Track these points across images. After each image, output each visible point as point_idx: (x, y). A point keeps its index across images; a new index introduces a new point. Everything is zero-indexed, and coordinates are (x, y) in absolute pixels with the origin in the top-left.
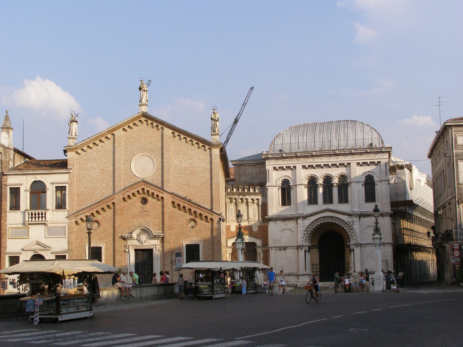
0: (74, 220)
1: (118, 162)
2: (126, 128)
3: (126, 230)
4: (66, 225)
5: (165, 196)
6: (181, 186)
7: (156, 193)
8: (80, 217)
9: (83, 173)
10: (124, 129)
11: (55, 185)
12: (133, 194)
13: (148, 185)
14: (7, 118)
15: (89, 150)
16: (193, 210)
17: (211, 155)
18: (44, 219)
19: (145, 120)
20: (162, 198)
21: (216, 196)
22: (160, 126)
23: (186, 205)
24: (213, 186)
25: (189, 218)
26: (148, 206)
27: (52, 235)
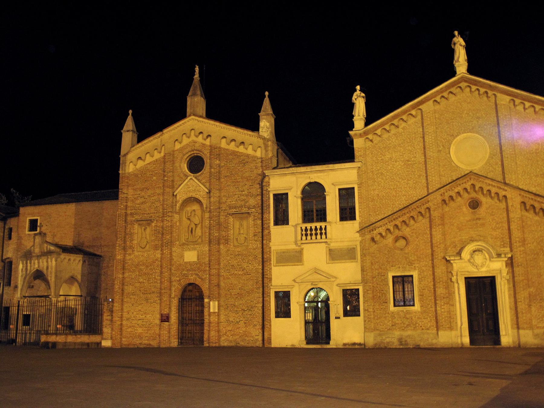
0: (368, 237)
1: (431, 147)
3: (450, 249)
4: (358, 243)
5: (510, 193)
7: (494, 190)
8: (377, 230)
9: (379, 168)
10: (435, 101)
15: (386, 135)
18: (324, 236)
20: (505, 197)
22: (490, 93)
26: (482, 211)
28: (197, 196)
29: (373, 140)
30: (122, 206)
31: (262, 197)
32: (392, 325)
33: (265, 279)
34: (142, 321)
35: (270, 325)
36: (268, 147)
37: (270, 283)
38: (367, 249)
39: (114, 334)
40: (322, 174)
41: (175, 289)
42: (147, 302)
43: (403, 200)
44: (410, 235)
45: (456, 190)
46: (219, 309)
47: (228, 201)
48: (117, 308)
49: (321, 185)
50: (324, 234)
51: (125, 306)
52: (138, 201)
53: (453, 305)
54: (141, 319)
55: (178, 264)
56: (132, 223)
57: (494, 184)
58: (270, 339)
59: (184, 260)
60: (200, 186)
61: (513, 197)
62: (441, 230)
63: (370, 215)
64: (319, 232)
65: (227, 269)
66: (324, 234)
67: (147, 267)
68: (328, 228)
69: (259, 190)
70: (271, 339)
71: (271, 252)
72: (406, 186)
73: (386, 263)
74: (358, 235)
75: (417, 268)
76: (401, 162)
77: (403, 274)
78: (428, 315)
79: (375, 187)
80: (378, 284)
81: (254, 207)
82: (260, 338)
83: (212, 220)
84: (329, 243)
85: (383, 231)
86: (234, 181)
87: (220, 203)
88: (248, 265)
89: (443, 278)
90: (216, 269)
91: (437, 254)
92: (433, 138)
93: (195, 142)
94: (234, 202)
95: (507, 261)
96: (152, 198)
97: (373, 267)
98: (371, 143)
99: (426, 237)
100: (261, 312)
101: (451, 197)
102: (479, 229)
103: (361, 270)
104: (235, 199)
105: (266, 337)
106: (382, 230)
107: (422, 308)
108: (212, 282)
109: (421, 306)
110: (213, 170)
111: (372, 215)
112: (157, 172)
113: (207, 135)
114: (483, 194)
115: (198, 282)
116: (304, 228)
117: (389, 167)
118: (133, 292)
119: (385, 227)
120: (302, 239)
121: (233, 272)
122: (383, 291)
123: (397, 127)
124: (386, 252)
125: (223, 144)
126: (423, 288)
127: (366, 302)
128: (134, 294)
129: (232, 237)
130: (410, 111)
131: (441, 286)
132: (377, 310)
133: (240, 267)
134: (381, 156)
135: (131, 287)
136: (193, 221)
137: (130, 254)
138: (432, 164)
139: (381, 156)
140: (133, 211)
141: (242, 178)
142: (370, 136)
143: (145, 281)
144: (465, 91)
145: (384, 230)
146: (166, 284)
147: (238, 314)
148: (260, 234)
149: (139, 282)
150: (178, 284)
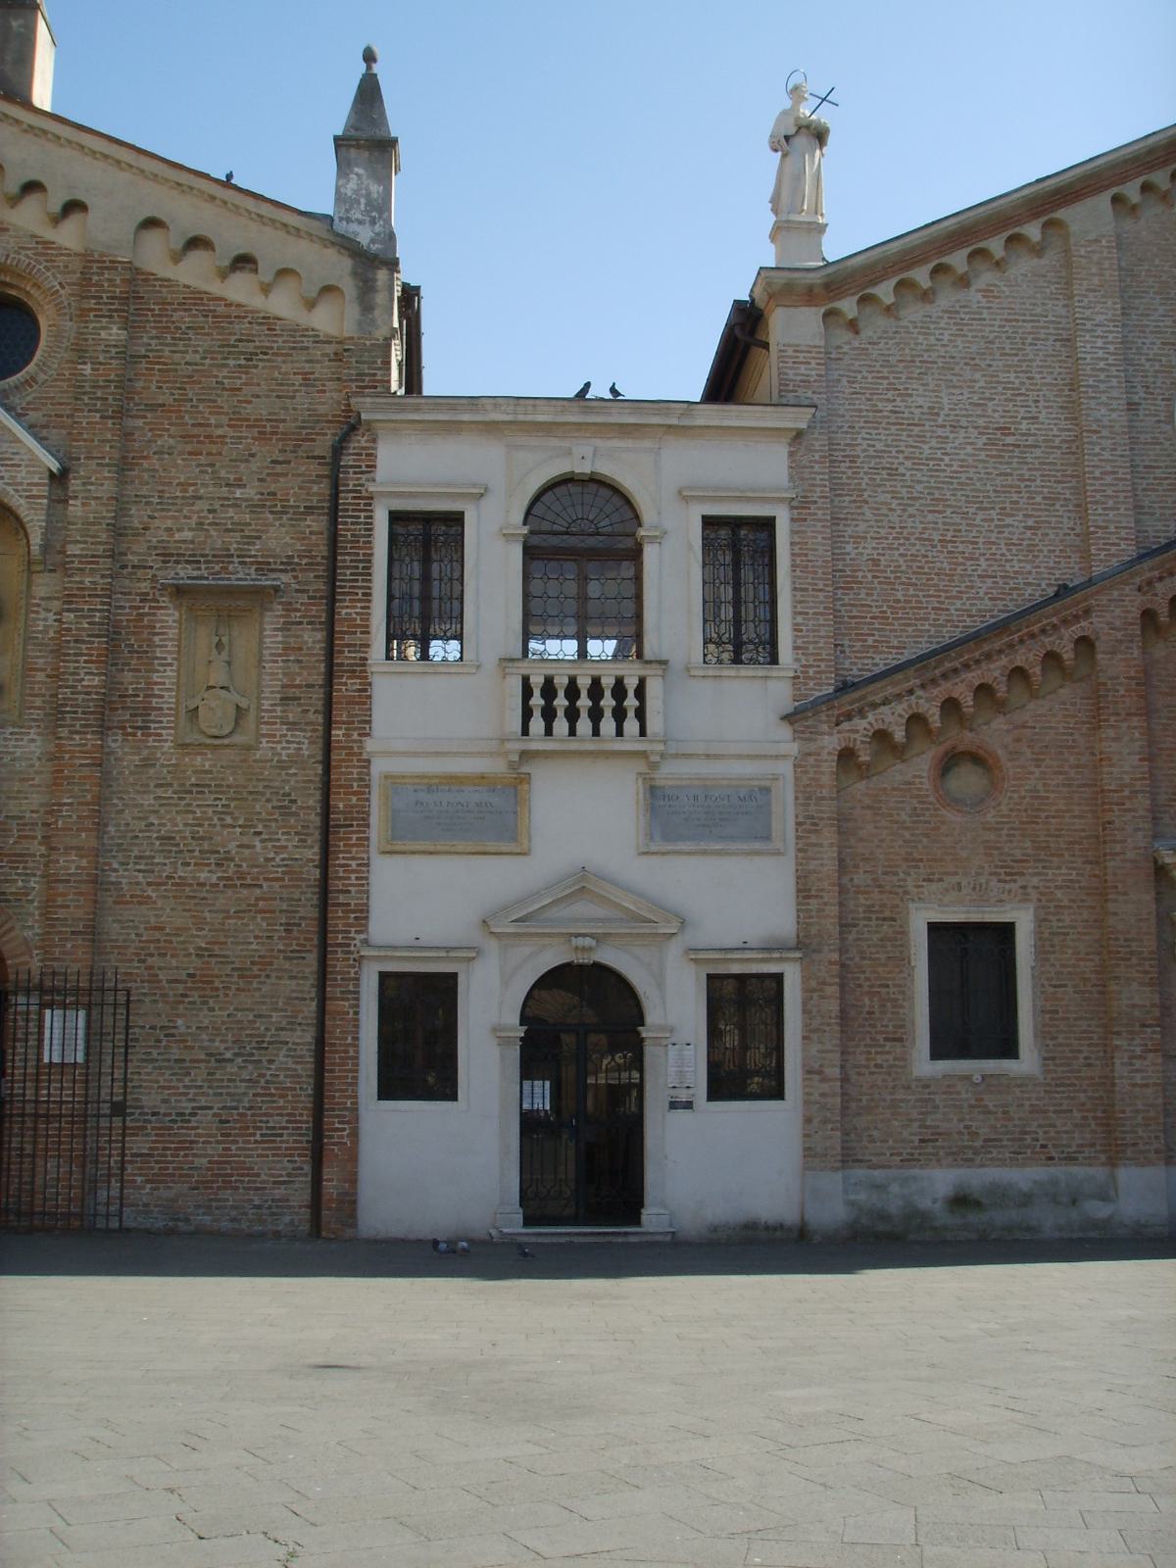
0: (831, 743)
1: (1102, 386)
4: (786, 769)
8: (871, 717)
9: (879, 446)
14: (369, 94)
18: (631, 725)
29: (861, 324)
31: (334, 521)
32: (922, 1141)
33: (336, 915)
35: (355, 1134)
36: (377, 291)
37: (357, 932)
38: (823, 798)
40: (629, 443)
43: (981, 594)
44: (1006, 747)
46: (87, 1054)
47: (157, 523)
49: (615, 490)
50: (631, 714)
58: (349, 1203)
60: (20, 441)
63: (836, 645)
64: (608, 702)
65: (136, 852)
66: (631, 714)
68: (653, 689)
69: (315, 488)
70: (355, 1202)
71: (368, 786)
72: (993, 537)
74: (785, 732)
75: (1034, 895)
76: (973, 433)
77: (975, 918)
78: (1072, 1098)
80: (864, 958)
82: (299, 1194)
83: (69, 610)
84: (653, 758)
86: (196, 431)
87: (118, 531)
88: (245, 840)
89: (1141, 940)
90: (78, 848)
91: (1118, 838)
92: (1111, 348)
94: (187, 535)
97: (845, 880)
99: (1072, 760)
100: (306, 1069)
103: (798, 891)
104: (195, 518)
105: (331, 1186)
106: (893, 718)
108: (61, 914)
111: (847, 650)
113: (67, 197)
116: (537, 681)
117: (926, 447)
119: (905, 705)
120: (525, 731)
121: (168, 870)
122: (888, 986)
124: (904, 817)
125: (154, 255)
126: (1054, 982)
127: (815, 1036)
129: (169, 699)
130: (1019, 223)
132: (859, 1074)
133: (206, 846)
134: (890, 395)
138: (1107, 455)
139: (890, 395)
142: (848, 306)
145: (900, 715)
148: (318, 695)
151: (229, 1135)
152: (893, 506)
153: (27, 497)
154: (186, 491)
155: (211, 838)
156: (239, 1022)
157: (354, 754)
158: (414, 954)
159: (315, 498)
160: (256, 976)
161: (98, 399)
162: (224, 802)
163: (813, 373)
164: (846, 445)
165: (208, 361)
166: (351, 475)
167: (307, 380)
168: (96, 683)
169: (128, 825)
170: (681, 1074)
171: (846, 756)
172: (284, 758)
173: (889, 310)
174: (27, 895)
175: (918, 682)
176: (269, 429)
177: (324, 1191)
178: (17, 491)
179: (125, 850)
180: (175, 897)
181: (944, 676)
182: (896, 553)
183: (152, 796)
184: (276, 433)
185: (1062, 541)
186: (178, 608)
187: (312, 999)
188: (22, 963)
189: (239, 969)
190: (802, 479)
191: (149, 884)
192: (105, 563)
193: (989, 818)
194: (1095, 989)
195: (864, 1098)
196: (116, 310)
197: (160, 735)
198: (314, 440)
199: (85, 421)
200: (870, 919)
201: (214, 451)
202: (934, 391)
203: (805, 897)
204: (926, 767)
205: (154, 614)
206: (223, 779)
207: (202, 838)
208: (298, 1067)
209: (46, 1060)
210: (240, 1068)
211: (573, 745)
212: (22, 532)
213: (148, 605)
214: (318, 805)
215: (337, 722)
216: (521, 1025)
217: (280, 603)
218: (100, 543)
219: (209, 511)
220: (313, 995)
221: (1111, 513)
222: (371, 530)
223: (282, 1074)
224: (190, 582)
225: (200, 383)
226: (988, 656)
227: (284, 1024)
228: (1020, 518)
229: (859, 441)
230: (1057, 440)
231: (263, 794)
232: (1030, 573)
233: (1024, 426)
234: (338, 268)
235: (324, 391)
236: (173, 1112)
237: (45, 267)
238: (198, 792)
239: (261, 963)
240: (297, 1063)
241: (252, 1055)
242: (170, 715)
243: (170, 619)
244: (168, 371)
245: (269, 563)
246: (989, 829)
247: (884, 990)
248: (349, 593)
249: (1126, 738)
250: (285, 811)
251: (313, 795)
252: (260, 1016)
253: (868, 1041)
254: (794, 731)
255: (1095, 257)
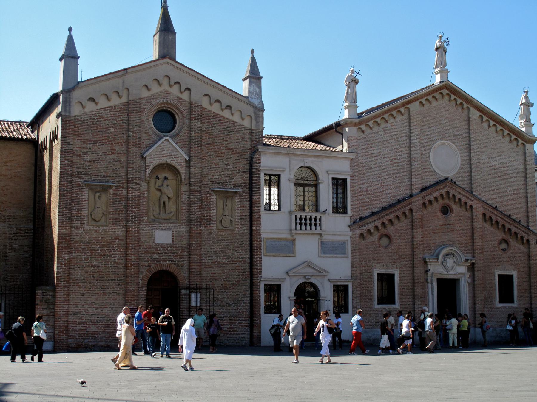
0: (358, 232)
1: (416, 149)
2: (423, 100)
4: (349, 238)
6: (491, 192)
7: (464, 199)
8: (367, 226)
9: (368, 161)
10: (421, 102)
11: (331, 177)
12: (436, 198)
13: (454, 188)
15: (376, 128)
16: (507, 226)
17: (525, 154)
18: (318, 228)
19: (448, 94)
20: (471, 206)
21: (532, 209)
22: (465, 106)
23: (499, 220)
24: (528, 195)
25: (500, 238)
26: (453, 217)
27: (328, 253)
28: (174, 163)
29: (365, 131)
30: (66, 162)
32: (376, 323)
34: (97, 316)
35: (260, 322)
39: (57, 334)
41: (143, 276)
42: (104, 292)
44: (393, 234)
45: (435, 195)
47: (210, 174)
48: (62, 299)
51: (71, 296)
52: (88, 158)
53: (427, 304)
54: (95, 314)
55: (146, 246)
56: (79, 186)
57: (464, 193)
58: (259, 338)
59: (154, 241)
60: (178, 151)
61: (477, 207)
62: (421, 232)
67: (103, 246)
68: (323, 219)
69: (246, 167)
70: (260, 337)
73: (372, 260)
74: (348, 229)
76: (388, 159)
79: (364, 181)
80: (364, 281)
81: (240, 186)
82: (247, 336)
83: (192, 195)
85: (372, 228)
86: (218, 150)
88: (233, 252)
90: (198, 254)
92: (418, 140)
93: (168, 93)
94: (217, 177)
95: (469, 265)
96: (109, 156)
98: (362, 134)
100: (248, 307)
101: (430, 201)
102: (450, 234)
103: (351, 266)
105: (255, 334)
106: (371, 226)
107: (402, 306)
108: (193, 270)
109: (401, 305)
110: (193, 133)
112: (115, 122)
114: (455, 202)
115: (173, 269)
116: (298, 216)
117: (378, 162)
118: (83, 278)
119: (373, 224)
120: (296, 229)
121: (216, 260)
123: (387, 122)
125: (205, 102)
126: (403, 287)
127: (355, 299)
128: (84, 281)
129: (214, 218)
131: (419, 286)
135: (80, 272)
136: (165, 194)
137: (77, 228)
138: (416, 166)
140: (80, 170)
141: (227, 149)
142: (363, 127)
143: (100, 265)
144: (445, 98)
146: (133, 270)
147: (222, 308)
148: (248, 218)
149: (92, 266)
150: (147, 271)
151: (231, 322)
152: (371, 176)
153: (181, 166)
154: (216, 166)
155: (225, 252)
156: (233, 296)
157: (258, 233)
158: (276, 280)
159: (246, 169)
160: (236, 285)
161: (196, 141)
162: (228, 243)
163: (355, 143)
164: (361, 161)
165: (220, 132)
166: (255, 164)
167: (243, 139)
168: (199, 214)
169: (206, 248)
170: (328, 307)
171: (362, 235)
172: (241, 233)
173: (371, 128)
174: (184, 265)
175: (376, 218)
176: (235, 151)
177: (254, 335)
178: (178, 164)
179: (206, 255)
180: (218, 266)
181: (382, 217)
182: (371, 187)
183: (212, 241)
184: (236, 152)
185: (406, 186)
186: (216, 195)
187: (249, 290)
188: (183, 282)
189: (233, 283)
190: (353, 170)
191: (212, 263)
192: (199, 184)
193: (390, 250)
194: (411, 289)
195: (364, 313)
196: (199, 118)
197: (213, 227)
198: (245, 154)
199: (193, 147)
200: (365, 272)
201: (222, 156)
202: (380, 148)
203: (353, 267)
204: (377, 238)
205: (210, 197)
206: (227, 238)
207: (223, 252)
208: (246, 306)
209: (192, 305)
210: (233, 307)
211: (301, 232)
212: (178, 175)
213: (209, 194)
214: (249, 244)
215: (254, 225)
216: (295, 296)
217: (239, 195)
218: (199, 179)
219: (222, 171)
220: (249, 289)
221: (417, 180)
222: (260, 178)
223: (243, 308)
224: (219, 189)
225: (218, 138)
226: (391, 213)
227: (243, 296)
228: (397, 180)
229: (364, 160)
230: (405, 161)
231: (237, 241)
232: (399, 193)
233: (398, 158)
234: (251, 111)
235: (247, 142)
236: (219, 317)
237: (180, 105)
238: (222, 241)
239: (238, 282)
240: (246, 305)
241: (236, 303)
242: (215, 222)
243: (214, 198)
244: (211, 134)
245: (236, 185)
246: (390, 252)
247: (368, 289)
248: (256, 194)
249: (418, 232)
250: (242, 245)
251: (247, 242)
252: (237, 294)
253: (365, 300)
254: (351, 229)
255: (415, 117)
